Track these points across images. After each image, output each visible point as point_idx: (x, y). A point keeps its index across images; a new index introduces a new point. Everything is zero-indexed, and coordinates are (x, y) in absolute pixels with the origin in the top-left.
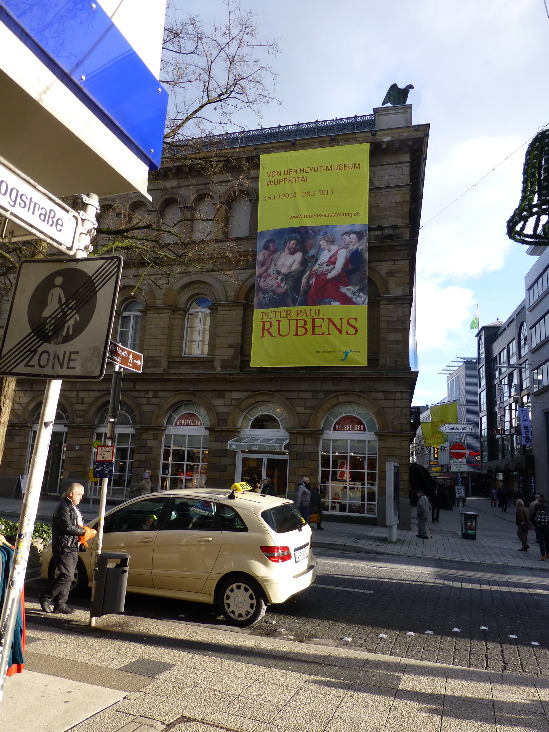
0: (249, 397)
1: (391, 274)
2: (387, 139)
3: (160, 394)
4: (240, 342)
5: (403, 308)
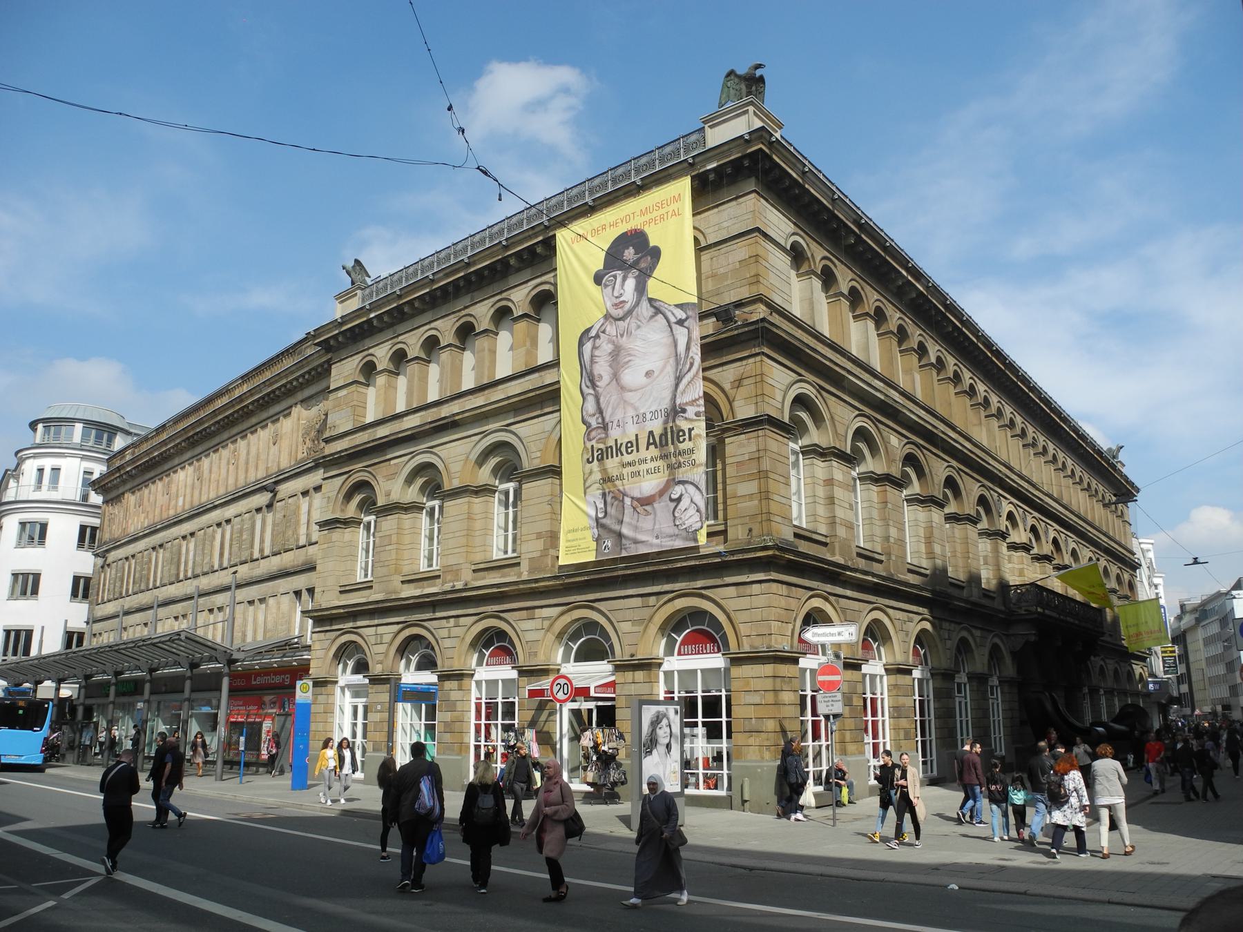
0: (562, 614)
1: (738, 383)
3: (462, 620)
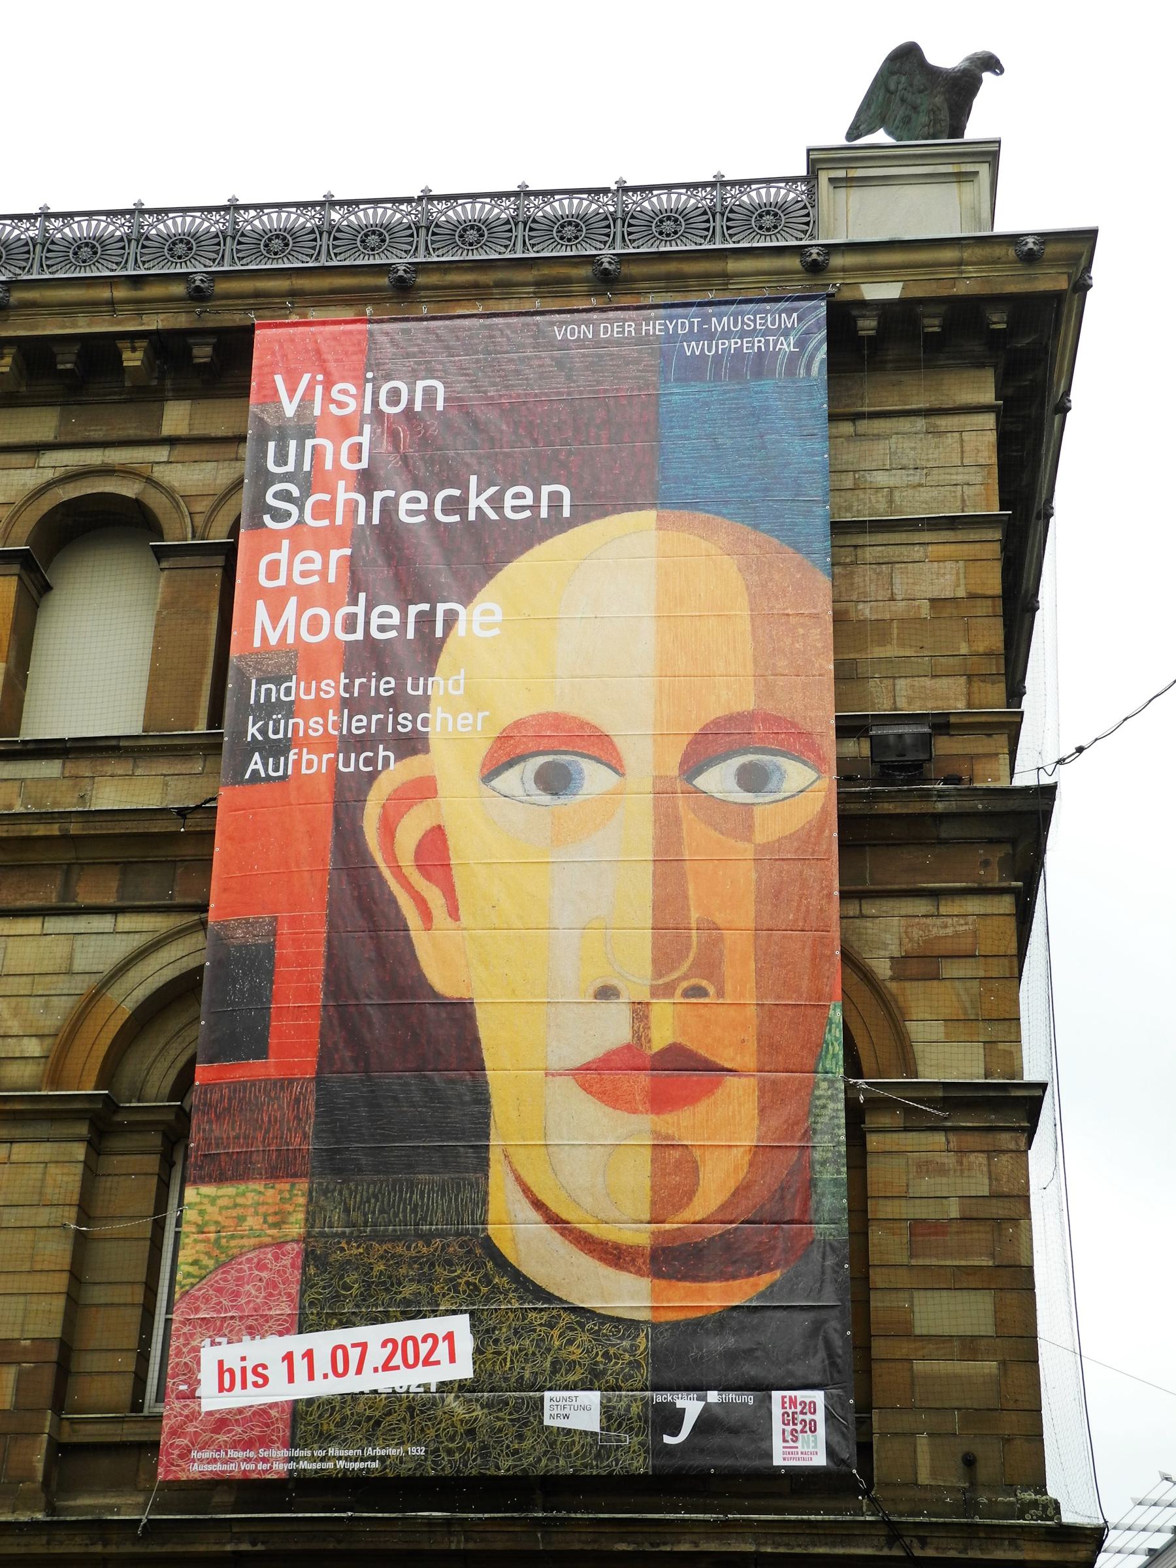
1: (922, 964)
2: (890, 291)
4: (55, 1331)
5: (991, 1153)
